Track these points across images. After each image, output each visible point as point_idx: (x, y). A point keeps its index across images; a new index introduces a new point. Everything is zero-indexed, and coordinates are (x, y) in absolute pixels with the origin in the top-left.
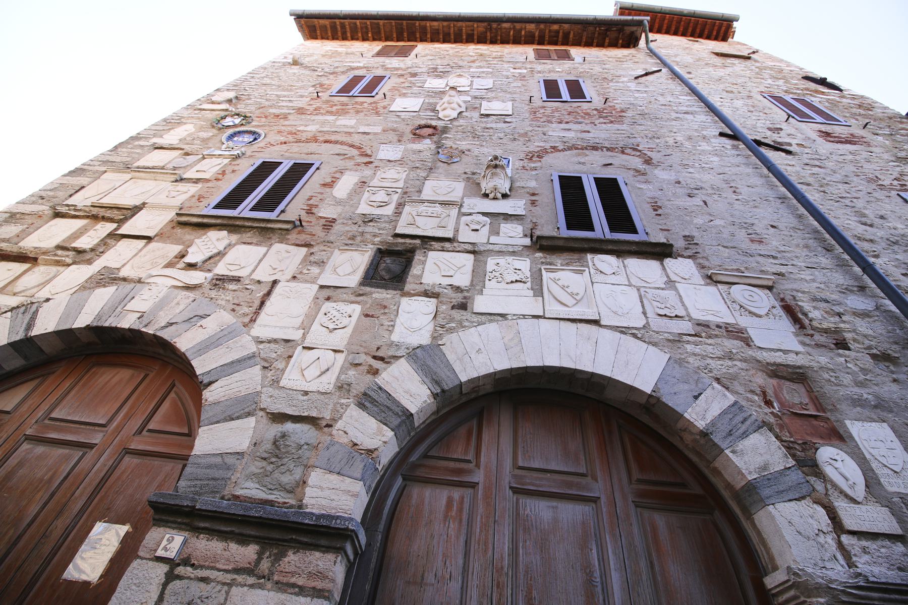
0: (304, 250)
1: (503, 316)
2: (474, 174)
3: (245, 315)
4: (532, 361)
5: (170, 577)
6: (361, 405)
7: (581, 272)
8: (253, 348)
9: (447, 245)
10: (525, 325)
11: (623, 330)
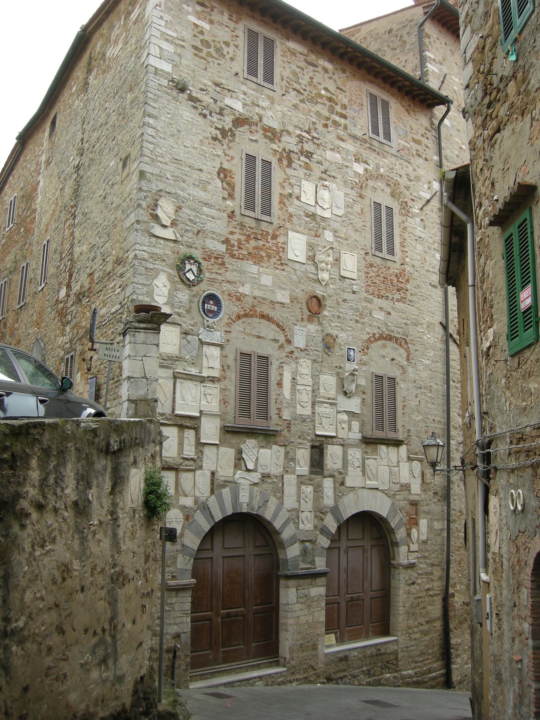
0: (284, 448)
1: (354, 487)
2: (340, 368)
3: (279, 498)
4: (361, 510)
5: (297, 590)
6: (321, 533)
7: (375, 459)
8: (288, 515)
9: (334, 440)
10: (360, 491)
11: (382, 491)
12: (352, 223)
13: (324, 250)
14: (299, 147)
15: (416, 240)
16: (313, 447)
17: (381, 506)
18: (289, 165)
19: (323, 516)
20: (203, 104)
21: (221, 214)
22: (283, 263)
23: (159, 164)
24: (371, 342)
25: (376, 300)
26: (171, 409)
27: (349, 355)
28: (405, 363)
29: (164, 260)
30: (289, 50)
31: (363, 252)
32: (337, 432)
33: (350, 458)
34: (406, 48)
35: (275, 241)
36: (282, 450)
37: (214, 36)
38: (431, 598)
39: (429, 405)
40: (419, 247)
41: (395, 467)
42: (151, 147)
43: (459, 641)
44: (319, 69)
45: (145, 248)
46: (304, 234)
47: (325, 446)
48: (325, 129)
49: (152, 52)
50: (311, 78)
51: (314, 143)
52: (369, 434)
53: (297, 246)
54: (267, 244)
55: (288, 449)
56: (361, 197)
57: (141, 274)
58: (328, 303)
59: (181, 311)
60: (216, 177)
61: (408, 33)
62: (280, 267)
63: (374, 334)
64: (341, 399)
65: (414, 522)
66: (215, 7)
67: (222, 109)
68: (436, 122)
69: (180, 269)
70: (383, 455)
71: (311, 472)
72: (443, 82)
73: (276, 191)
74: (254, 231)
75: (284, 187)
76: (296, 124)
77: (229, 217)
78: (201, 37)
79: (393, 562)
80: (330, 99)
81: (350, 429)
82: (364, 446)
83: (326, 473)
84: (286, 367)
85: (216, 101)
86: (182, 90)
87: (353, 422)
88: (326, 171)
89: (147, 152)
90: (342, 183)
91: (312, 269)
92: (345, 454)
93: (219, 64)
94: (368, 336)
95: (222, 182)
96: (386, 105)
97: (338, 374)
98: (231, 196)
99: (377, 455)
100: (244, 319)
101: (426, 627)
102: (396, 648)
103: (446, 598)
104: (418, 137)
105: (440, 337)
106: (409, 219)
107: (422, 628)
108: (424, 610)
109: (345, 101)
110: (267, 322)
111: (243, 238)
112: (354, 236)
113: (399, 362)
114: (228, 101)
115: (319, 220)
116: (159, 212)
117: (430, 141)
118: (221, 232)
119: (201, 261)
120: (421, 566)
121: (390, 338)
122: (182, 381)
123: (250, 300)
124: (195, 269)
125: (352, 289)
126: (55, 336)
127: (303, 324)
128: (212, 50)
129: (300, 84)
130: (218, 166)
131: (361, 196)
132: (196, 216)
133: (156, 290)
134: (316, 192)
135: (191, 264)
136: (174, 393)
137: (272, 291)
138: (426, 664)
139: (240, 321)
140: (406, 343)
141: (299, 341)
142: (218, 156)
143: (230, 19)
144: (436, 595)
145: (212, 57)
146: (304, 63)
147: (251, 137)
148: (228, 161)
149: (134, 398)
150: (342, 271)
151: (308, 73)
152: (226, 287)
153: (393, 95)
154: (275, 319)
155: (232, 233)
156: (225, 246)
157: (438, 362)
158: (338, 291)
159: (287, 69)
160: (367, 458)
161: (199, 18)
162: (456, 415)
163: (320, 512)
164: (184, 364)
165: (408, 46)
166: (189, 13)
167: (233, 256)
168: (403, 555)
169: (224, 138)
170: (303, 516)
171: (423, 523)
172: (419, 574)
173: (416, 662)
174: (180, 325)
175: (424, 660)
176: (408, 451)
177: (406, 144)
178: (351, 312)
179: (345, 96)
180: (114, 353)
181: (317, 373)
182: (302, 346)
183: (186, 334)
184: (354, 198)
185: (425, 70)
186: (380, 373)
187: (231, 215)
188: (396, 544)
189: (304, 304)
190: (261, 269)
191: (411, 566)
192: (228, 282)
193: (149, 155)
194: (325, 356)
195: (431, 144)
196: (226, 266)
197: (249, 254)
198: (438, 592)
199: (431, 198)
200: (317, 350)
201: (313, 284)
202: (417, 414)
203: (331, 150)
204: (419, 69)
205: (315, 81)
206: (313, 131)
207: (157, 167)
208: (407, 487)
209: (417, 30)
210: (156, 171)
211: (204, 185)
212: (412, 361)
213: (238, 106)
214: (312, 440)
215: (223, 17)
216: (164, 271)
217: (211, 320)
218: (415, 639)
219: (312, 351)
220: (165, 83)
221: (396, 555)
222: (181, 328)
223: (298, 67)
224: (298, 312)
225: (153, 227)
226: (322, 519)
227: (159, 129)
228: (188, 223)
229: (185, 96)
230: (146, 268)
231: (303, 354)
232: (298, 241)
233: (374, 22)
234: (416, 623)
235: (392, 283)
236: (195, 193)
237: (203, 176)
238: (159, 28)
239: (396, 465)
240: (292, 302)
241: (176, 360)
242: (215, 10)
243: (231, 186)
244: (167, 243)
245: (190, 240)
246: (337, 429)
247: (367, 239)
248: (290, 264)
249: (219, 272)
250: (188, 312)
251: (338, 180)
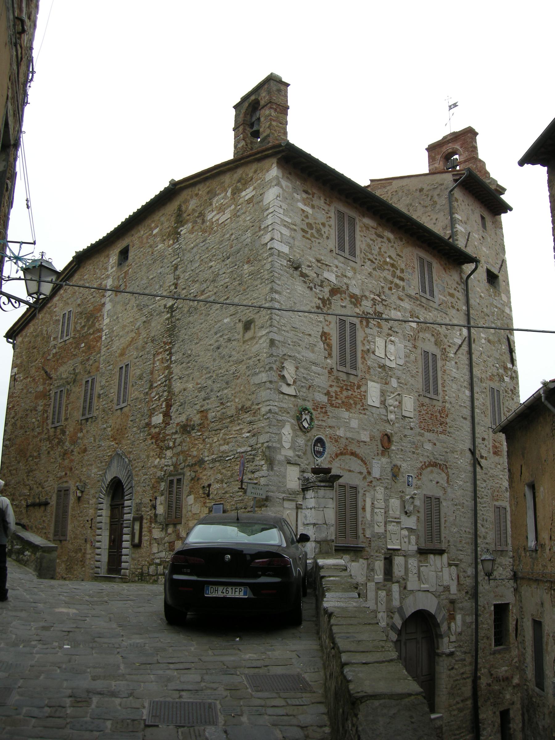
0: (366, 561)
1: (413, 591)
2: (403, 492)
6: (391, 629)
9: (399, 552)
12: (409, 371)
13: (393, 396)
14: (373, 309)
15: (452, 380)
16: (385, 559)
17: (430, 604)
18: (367, 326)
19: (393, 616)
20: (310, 278)
21: (324, 370)
22: (365, 408)
23: (283, 332)
24: (423, 469)
25: (426, 434)
27: (409, 482)
28: (446, 485)
29: (288, 413)
30: (365, 226)
31: (416, 395)
32: (401, 546)
33: (410, 566)
34: (437, 208)
35: (359, 391)
36: (365, 562)
37: (315, 219)
38: (464, 681)
39: (463, 519)
40: (454, 386)
41: (440, 572)
42: (278, 318)
43: (485, 716)
44: (385, 240)
45: (276, 404)
46: (378, 383)
47: (393, 557)
48: (390, 292)
49: (276, 237)
50: (380, 248)
51: (383, 305)
52: (423, 546)
53: (373, 392)
54: (354, 393)
55: (369, 561)
56: (415, 347)
57: (274, 426)
58: (395, 439)
60: (319, 340)
61: (438, 195)
62: (363, 412)
63: (425, 462)
64: (404, 518)
65: (452, 617)
66: (315, 193)
67: (322, 282)
68: (465, 277)
69: (299, 419)
70: (432, 563)
71: (385, 580)
72: (468, 240)
73: (360, 348)
74: (346, 383)
75: (364, 344)
76: (371, 289)
77: (329, 373)
78: (307, 221)
79: (439, 651)
80: (393, 265)
81: (409, 542)
82: (418, 555)
83: (394, 579)
84: (368, 494)
85: (318, 275)
86: (296, 269)
87: (411, 537)
88: (391, 327)
89: (275, 323)
90: (402, 337)
91: (383, 411)
92: (406, 562)
93: (319, 243)
94: (421, 465)
95: (324, 344)
96: (430, 265)
97: (401, 497)
98: (330, 355)
99: (427, 562)
100: (340, 457)
101: (461, 705)
102: (441, 723)
103: (475, 680)
104: (452, 291)
105: (468, 461)
106: (447, 363)
107: (458, 706)
108: (459, 691)
109: (403, 266)
111: (338, 389)
112: (412, 381)
113: (442, 484)
114: (326, 275)
115: (387, 370)
116: (285, 373)
117: (460, 294)
118: (324, 386)
119: (312, 411)
120: (457, 653)
121: (435, 465)
123: (344, 441)
124: (308, 418)
125: (410, 426)
126: (148, 457)
127: (379, 458)
128: (314, 231)
129: (372, 254)
130: (321, 330)
131: (415, 347)
132: (308, 374)
133: (284, 438)
134: (386, 346)
135: (306, 414)
136: (297, 521)
137: (358, 432)
138: (461, 737)
140: (447, 468)
141: (376, 473)
142: (320, 322)
143: (325, 203)
144: (468, 678)
145: (314, 237)
146: (375, 236)
147: (342, 304)
148: (327, 325)
149: (319, 540)
150: (403, 412)
151: (377, 244)
152: (328, 431)
153: (434, 256)
154: (360, 455)
155: (331, 386)
156: (327, 397)
157: (467, 482)
158: (401, 428)
159: (364, 242)
160: (422, 566)
161: (305, 205)
162: (480, 526)
163: (390, 612)
165: (438, 207)
166: (298, 201)
167: (332, 405)
168: (446, 646)
169: (324, 306)
170: (380, 615)
171: (459, 617)
172: (456, 661)
173: (455, 735)
174: (299, 465)
175: (460, 733)
176: (448, 558)
177: (444, 298)
178: (409, 445)
179: (403, 261)
180: (258, 491)
181: (388, 498)
182: (378, 476)
183: (303, 472)
184: (410, 349)
185: (455, 230)
186: (429, 494)
187: (331, 371)
188: (441, 636)
189: (379, 441)
190: (351, 415)
191: (452, 654)
192: (330, 427)
193: (277, 325)
194: (393, 483)
195: (460, 295)
196: (328, 414)
197: (343, 402)
198: (469, 675)
199: (462, 343)
200: (388, 479)
201: (385, 424)
202: (454, 527)
203: (395, 309)
204: (449, 228)
205: (382, 250)
206: (382, 294)
207: (282, 335)
208: (447, 589)
209: (447, 193)
210: (281, 339)
211: (312, 347)
212: (450, 483)
213: (332, 278)
214: (385, 553)
215: (320, 202)
216: (288, 421)
218: (454, 716)
219: (384, 479)
220: (285, 263)
221: (440, 645)
222: (300, 468)
223: (371, 240)
224: (376, 447)
225: (281, 386)
226: (392, 618)
227: (282, 302)
228: (303, 380)
229: (298, 273)
230: (277, 420)
231: (378, 482)
232: (374, 389)
233: (405, 179)
234: (455, 702)
235: (436, 419)
236: (307, 355)
237: (312, 340)
238: (279, 215)
239: (440, 570)
240: (371, 440)
241: (298, 494)
242: (315, 195)
243: (330, 346)
244: (290, 398)
245: (305, 394)
246: (401, 543)
247: (419, 383)
248: (369, 408)
249: (324, 419)
250: (304, 454)
251: (399, 335)
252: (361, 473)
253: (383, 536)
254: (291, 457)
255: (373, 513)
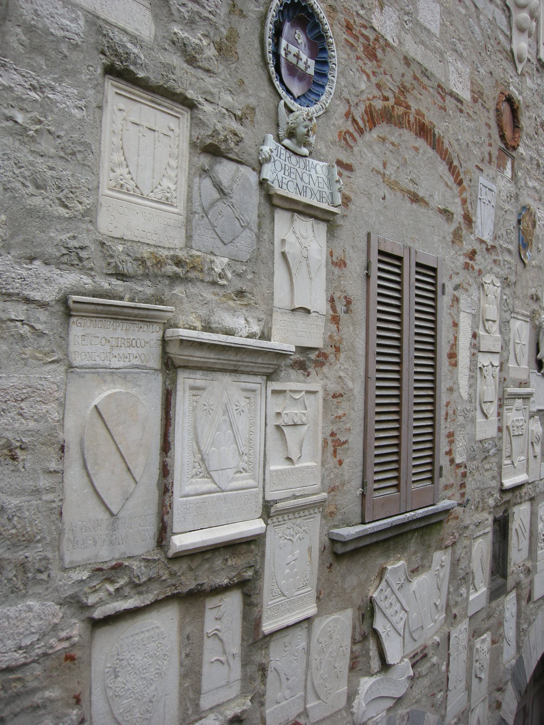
26: (150, 529)
59: (194, 38)
100: (382, 129)
110: (431, 152)
122: (198, 379)
136: (166, 446)
139: (375, 134)
164: (208, 294)
174: (190, 105)
183: (213, 151)
217: (301, 111)
222: (197, 122)
241: (174, 279)
250: (225, 49)
252: (446, 213)
253: (490, 453)
254: (135, 39)
255: (476, 370)
